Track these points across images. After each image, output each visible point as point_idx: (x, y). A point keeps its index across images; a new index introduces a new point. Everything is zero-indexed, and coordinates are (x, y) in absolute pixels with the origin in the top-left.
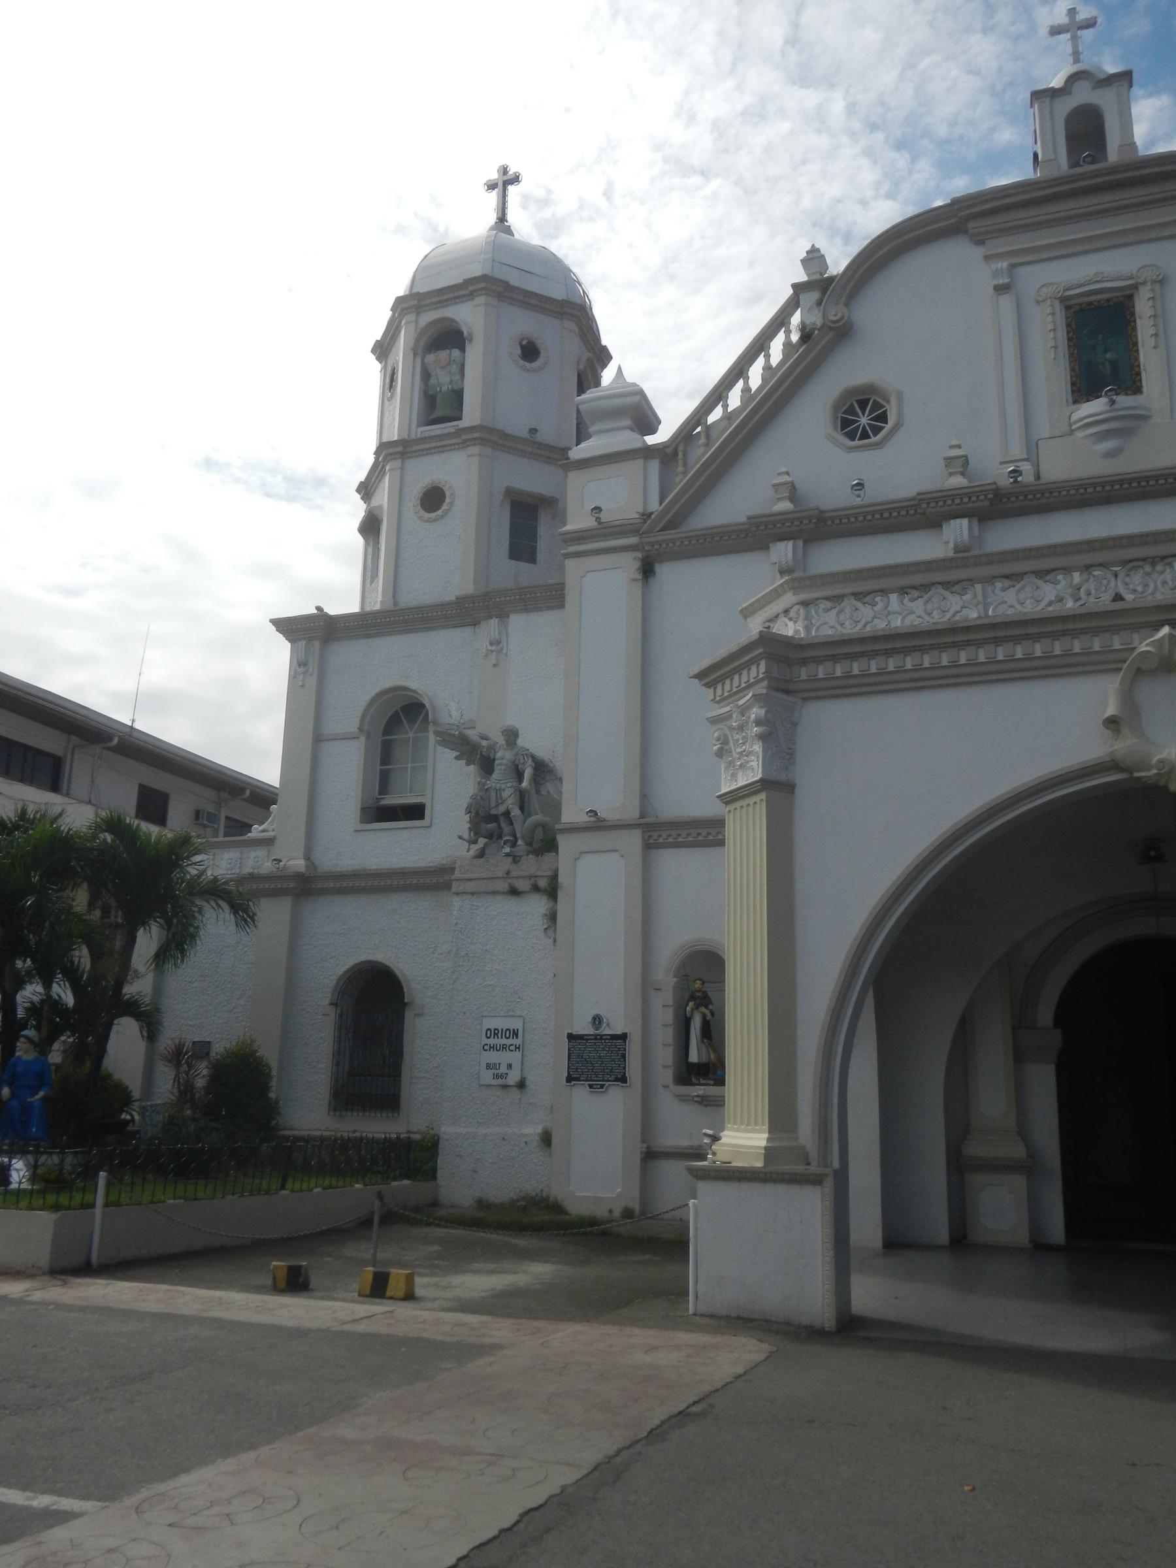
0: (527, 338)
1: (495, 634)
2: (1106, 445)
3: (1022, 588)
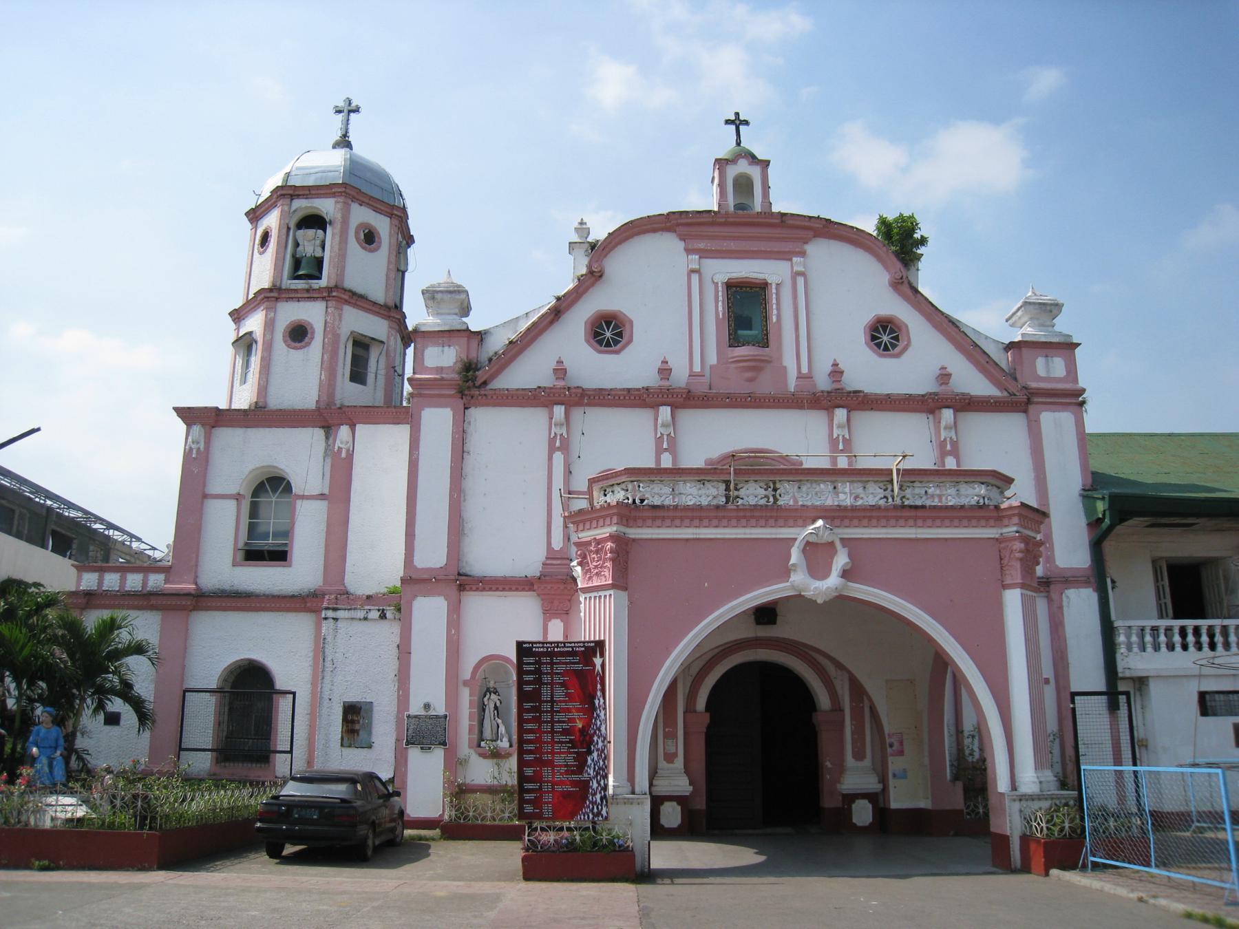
2: (749, 374)
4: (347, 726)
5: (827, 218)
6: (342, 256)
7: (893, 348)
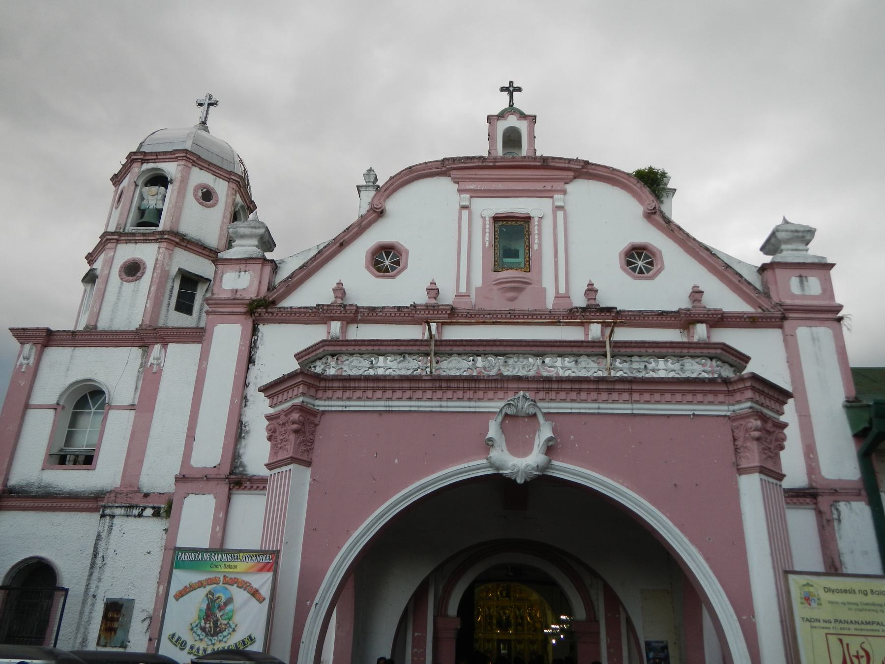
0: (206, 188)
1: (157, 354)
2: (511, 294)
3: (450, 362)
4: (106, 624)
5: (585, 160)
6: (178, 208)
7: (648, 272)
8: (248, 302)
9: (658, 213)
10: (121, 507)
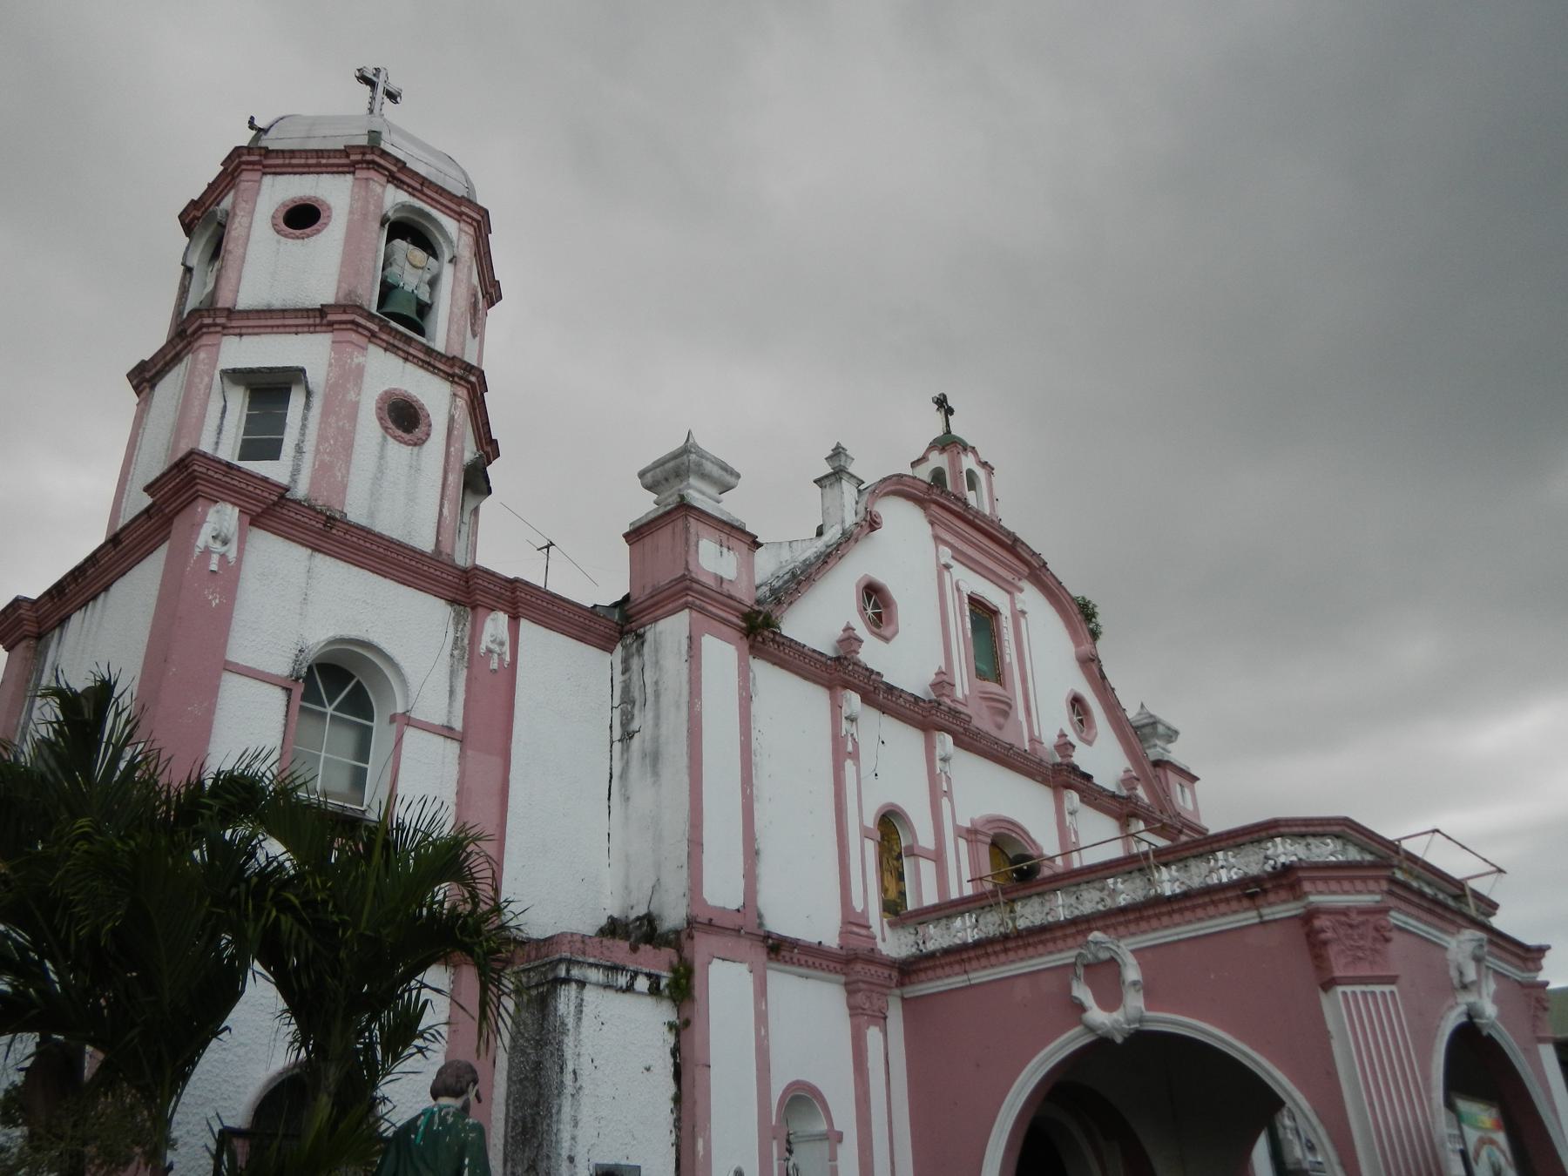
8: (747, 610)
9: (1096, 662)
10: (597, 966)
